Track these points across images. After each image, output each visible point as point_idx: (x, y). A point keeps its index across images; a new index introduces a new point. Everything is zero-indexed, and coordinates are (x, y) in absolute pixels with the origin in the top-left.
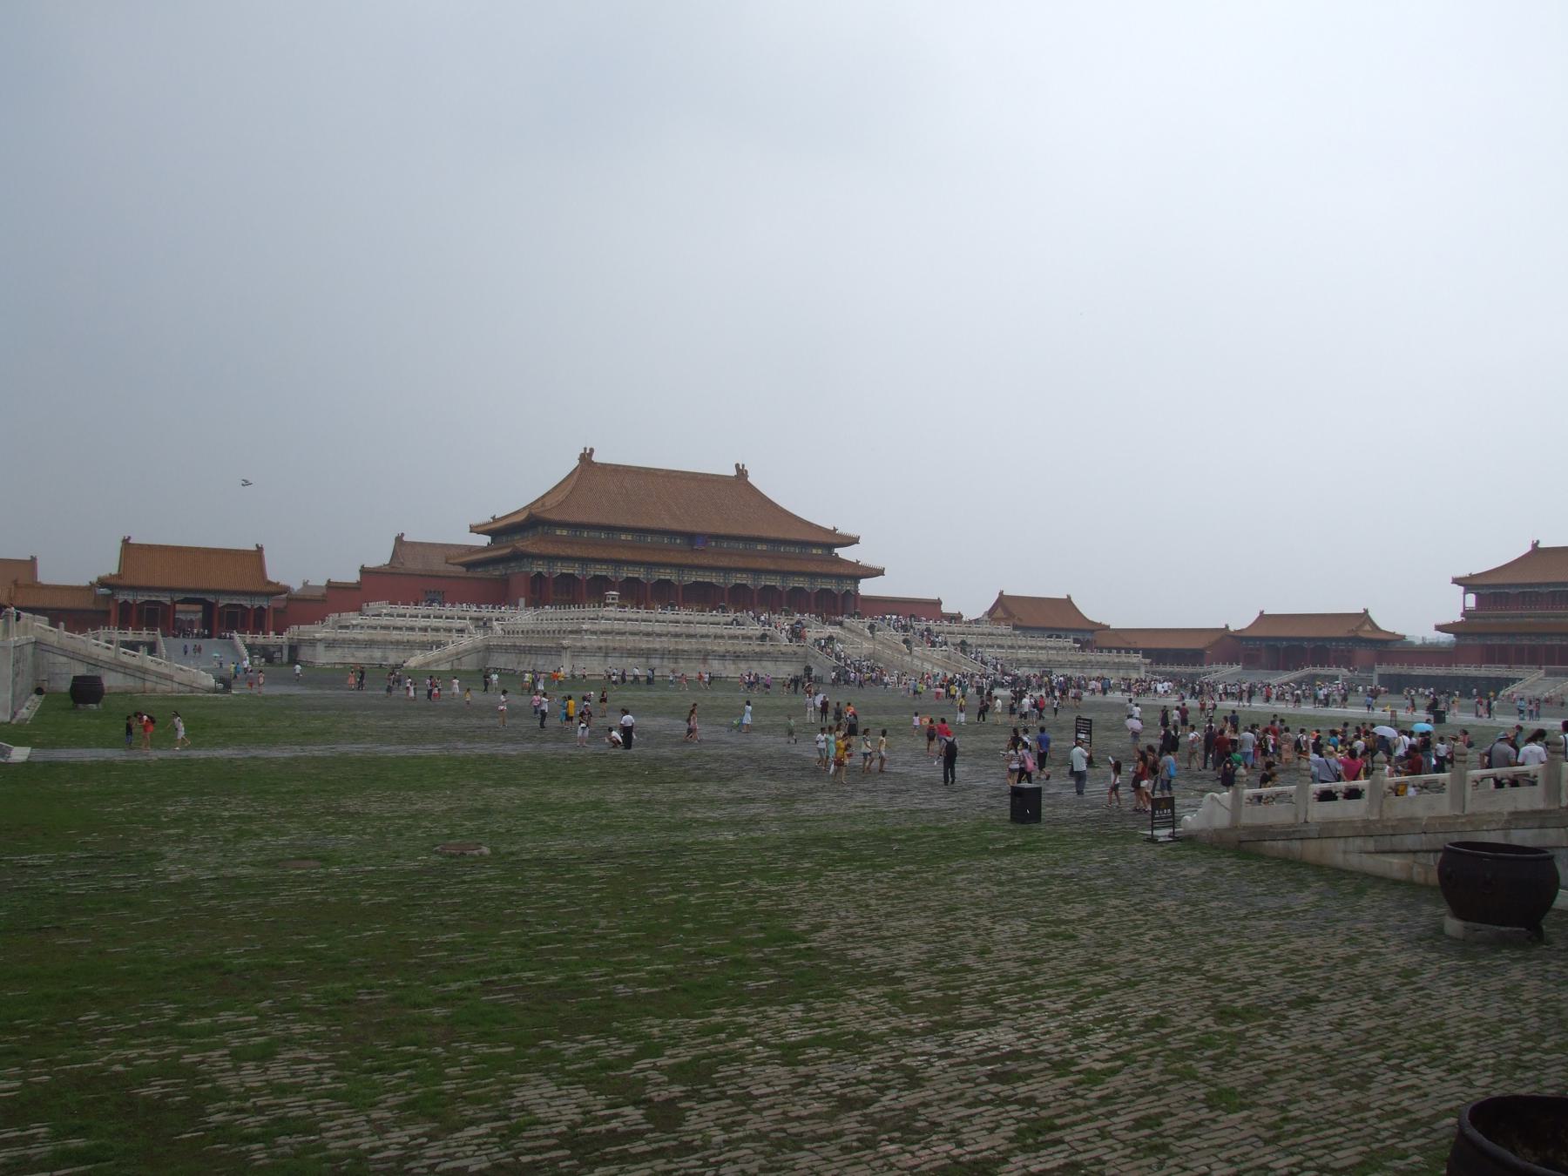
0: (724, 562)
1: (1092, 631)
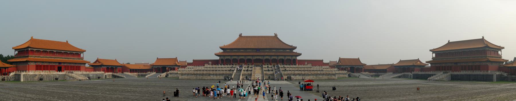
0: (263, 54)
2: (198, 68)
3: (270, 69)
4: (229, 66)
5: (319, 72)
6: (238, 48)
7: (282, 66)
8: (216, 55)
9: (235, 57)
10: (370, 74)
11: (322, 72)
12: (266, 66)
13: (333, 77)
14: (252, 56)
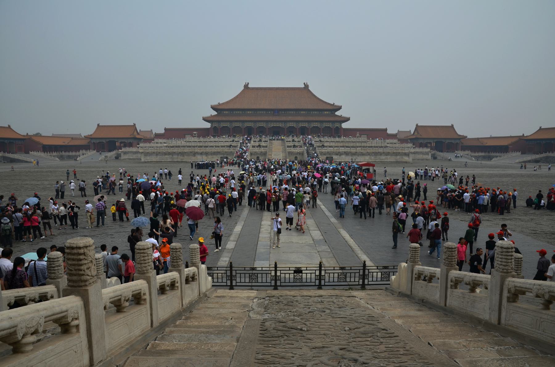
0: (284, 118)
1: (459, 139)
2: (174, 142)
3: (296, 144)
4: (227, 139)
5: (381, 150)
6: (242, 107)
7: (317, 139)
8: (205, 119)
9: (237, 124)
10: (473, 154)
11: (387, 150)
12: (290, 139)
13: (406, 159)
14: (267, 122)
